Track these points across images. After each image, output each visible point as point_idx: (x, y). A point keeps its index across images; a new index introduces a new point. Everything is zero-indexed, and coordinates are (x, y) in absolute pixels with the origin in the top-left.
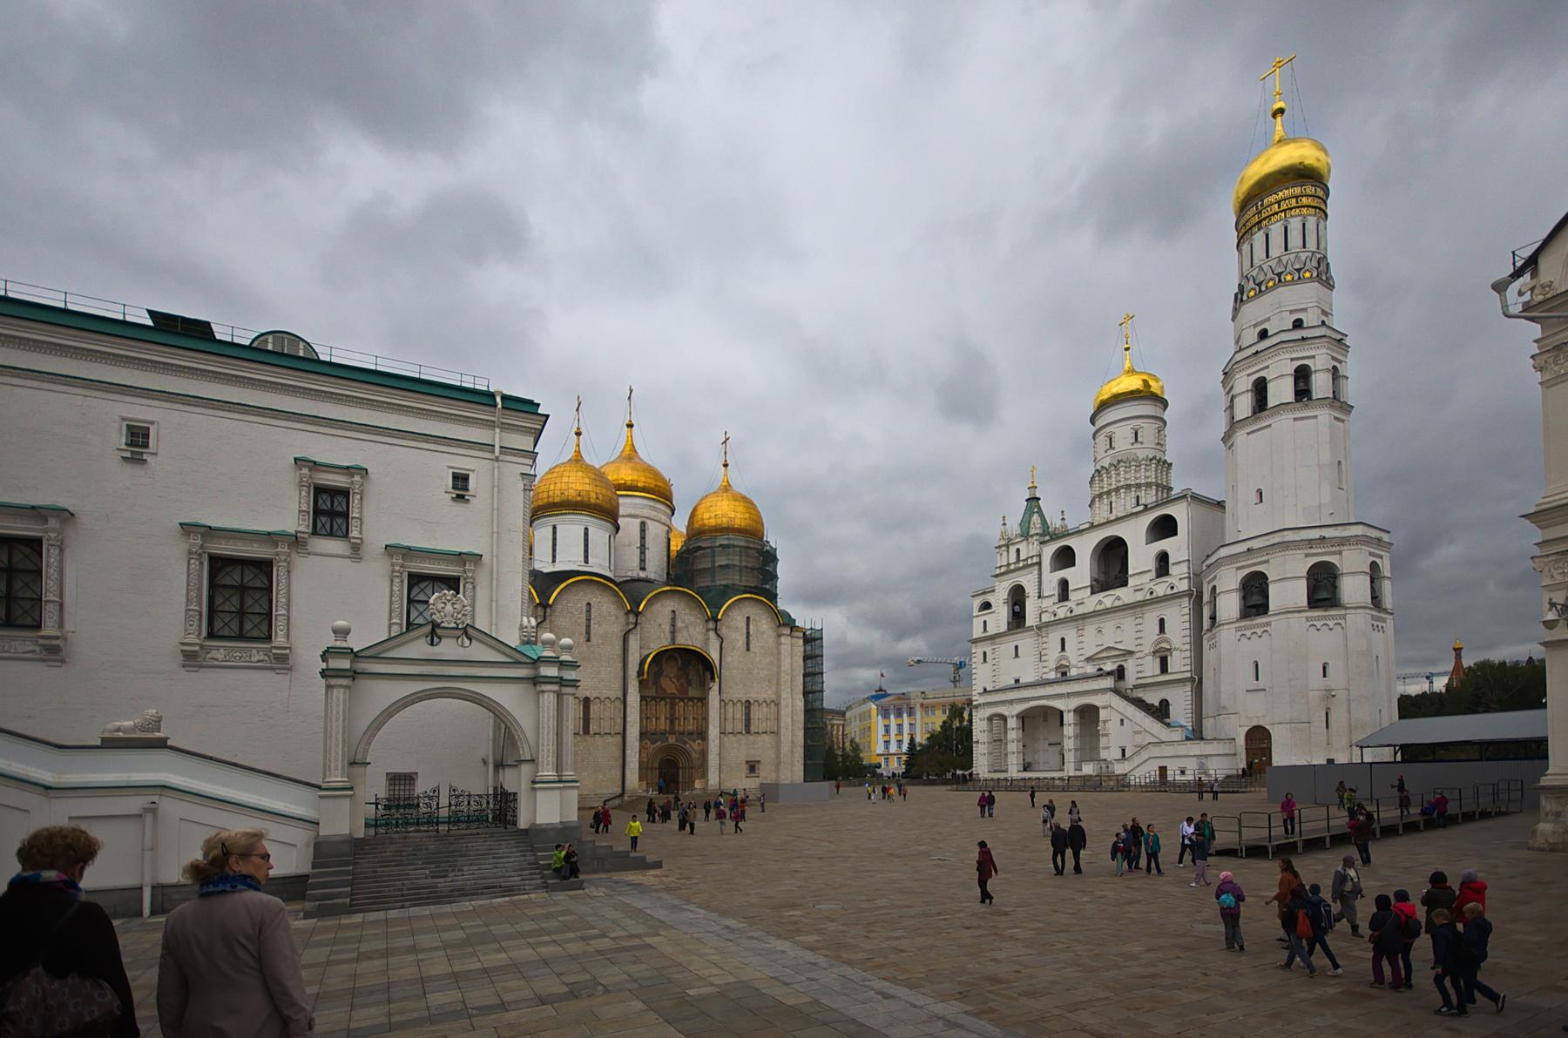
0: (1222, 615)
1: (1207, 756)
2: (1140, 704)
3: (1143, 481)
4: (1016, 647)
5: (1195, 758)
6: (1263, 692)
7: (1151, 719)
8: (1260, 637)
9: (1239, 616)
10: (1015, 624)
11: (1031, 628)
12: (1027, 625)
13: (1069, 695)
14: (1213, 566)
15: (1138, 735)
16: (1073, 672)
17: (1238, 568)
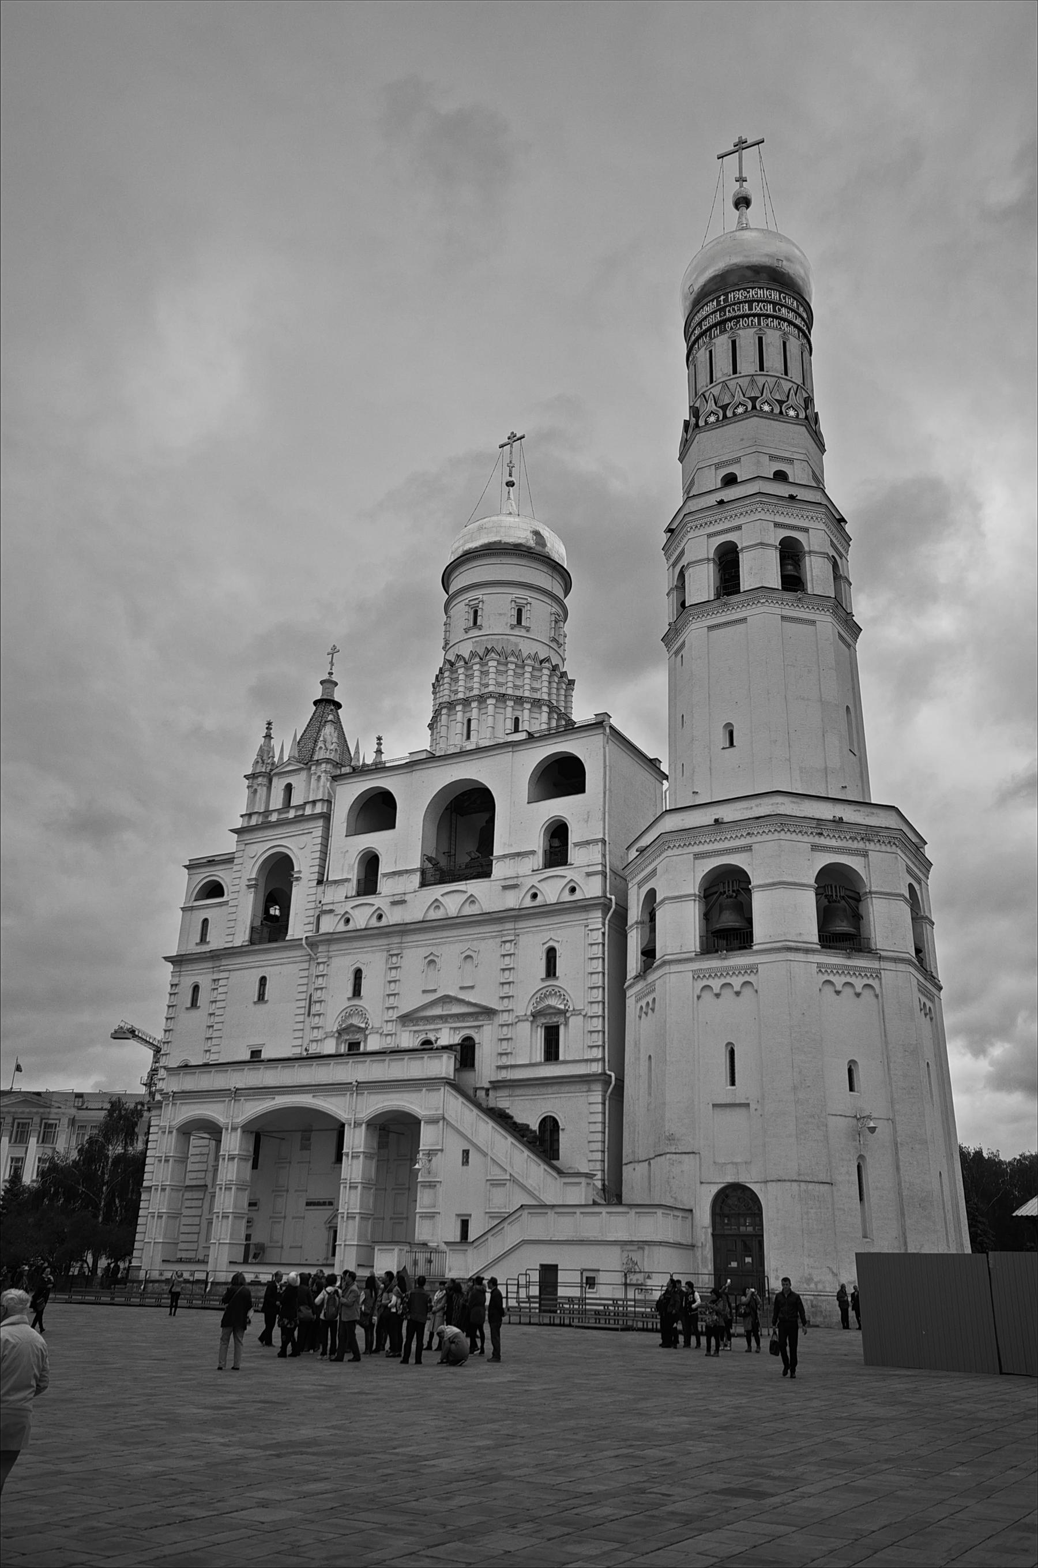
0: (663, 947)
1: (642, 1245)
2: (502, 1118)
3: (527, 694)
4: (263, 980)
5: (616, 1250)
6: (743, 1111)
7: (527, 1152)
9: (698, 950)
10: (266, 935)
11: (296, 944)
12: (287, 938)
13: (361, 1087)
14: (650, 850)
15: (500, 1189)
16: (373, 1043)
17: (697, 856)
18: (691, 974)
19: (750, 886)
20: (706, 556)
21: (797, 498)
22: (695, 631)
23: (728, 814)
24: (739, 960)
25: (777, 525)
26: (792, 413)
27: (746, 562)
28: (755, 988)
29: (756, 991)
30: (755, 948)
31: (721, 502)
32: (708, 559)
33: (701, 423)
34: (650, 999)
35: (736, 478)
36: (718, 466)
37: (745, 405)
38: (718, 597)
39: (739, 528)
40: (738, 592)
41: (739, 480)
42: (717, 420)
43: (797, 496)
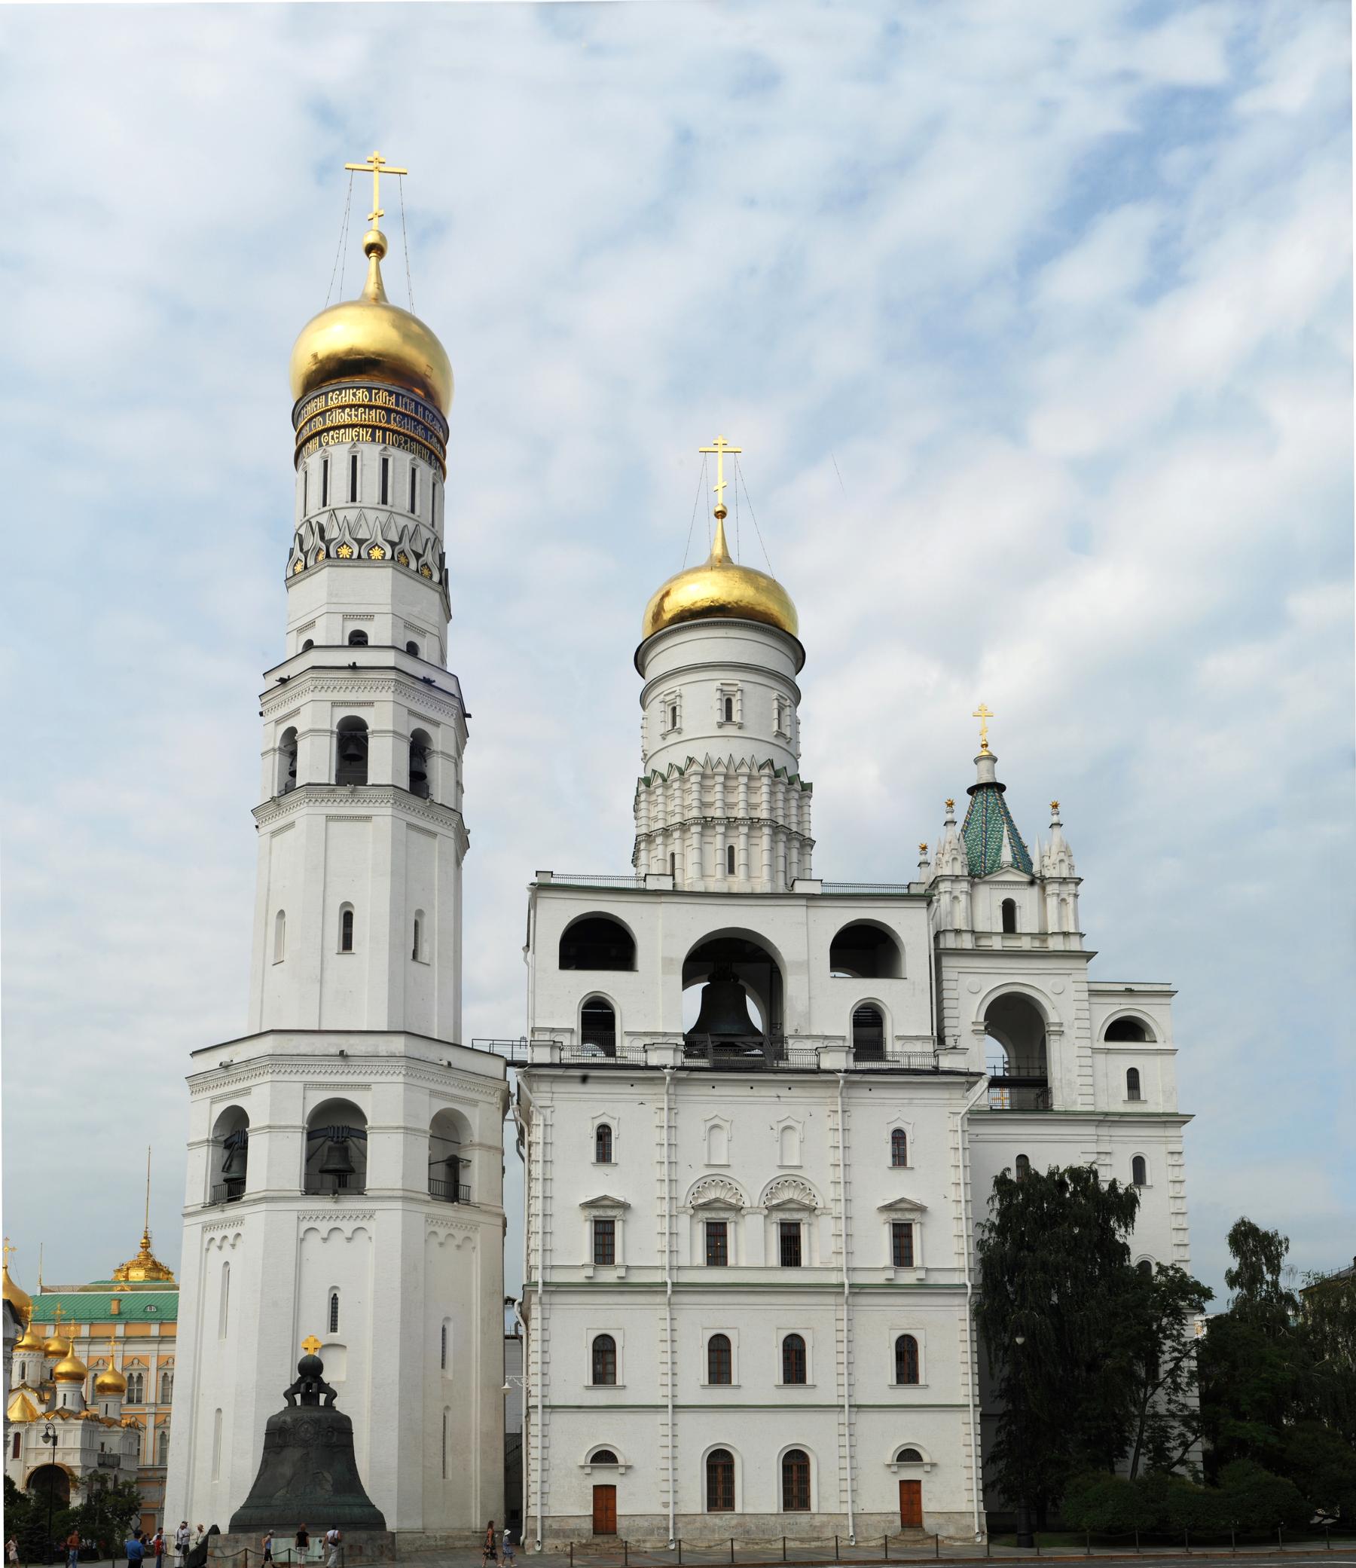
8: (349, 1239)
18: (295, 1215)
19: (366, 1126)
20: (327, 727)
21: (433, 684)
22: (304, 815)
23: (355, 1046)
24: (350, 1204)
25: (412, 713)
26: (426, 572)
27: (373, 744)
28: (370, 1235)
29: (370, 1238)
30: (369, 1193)
31: (354, 667)
32: (332, 732)
33: (333, 554)
34: (231, 1233)
35: (367, 642)
36: (347, 617)
37: (382, 549)
38: (338, 784)
39: (370, 704)
40: (363, 780)
41: (369, 644)
42: (350, 558)
43: (434, 681)
